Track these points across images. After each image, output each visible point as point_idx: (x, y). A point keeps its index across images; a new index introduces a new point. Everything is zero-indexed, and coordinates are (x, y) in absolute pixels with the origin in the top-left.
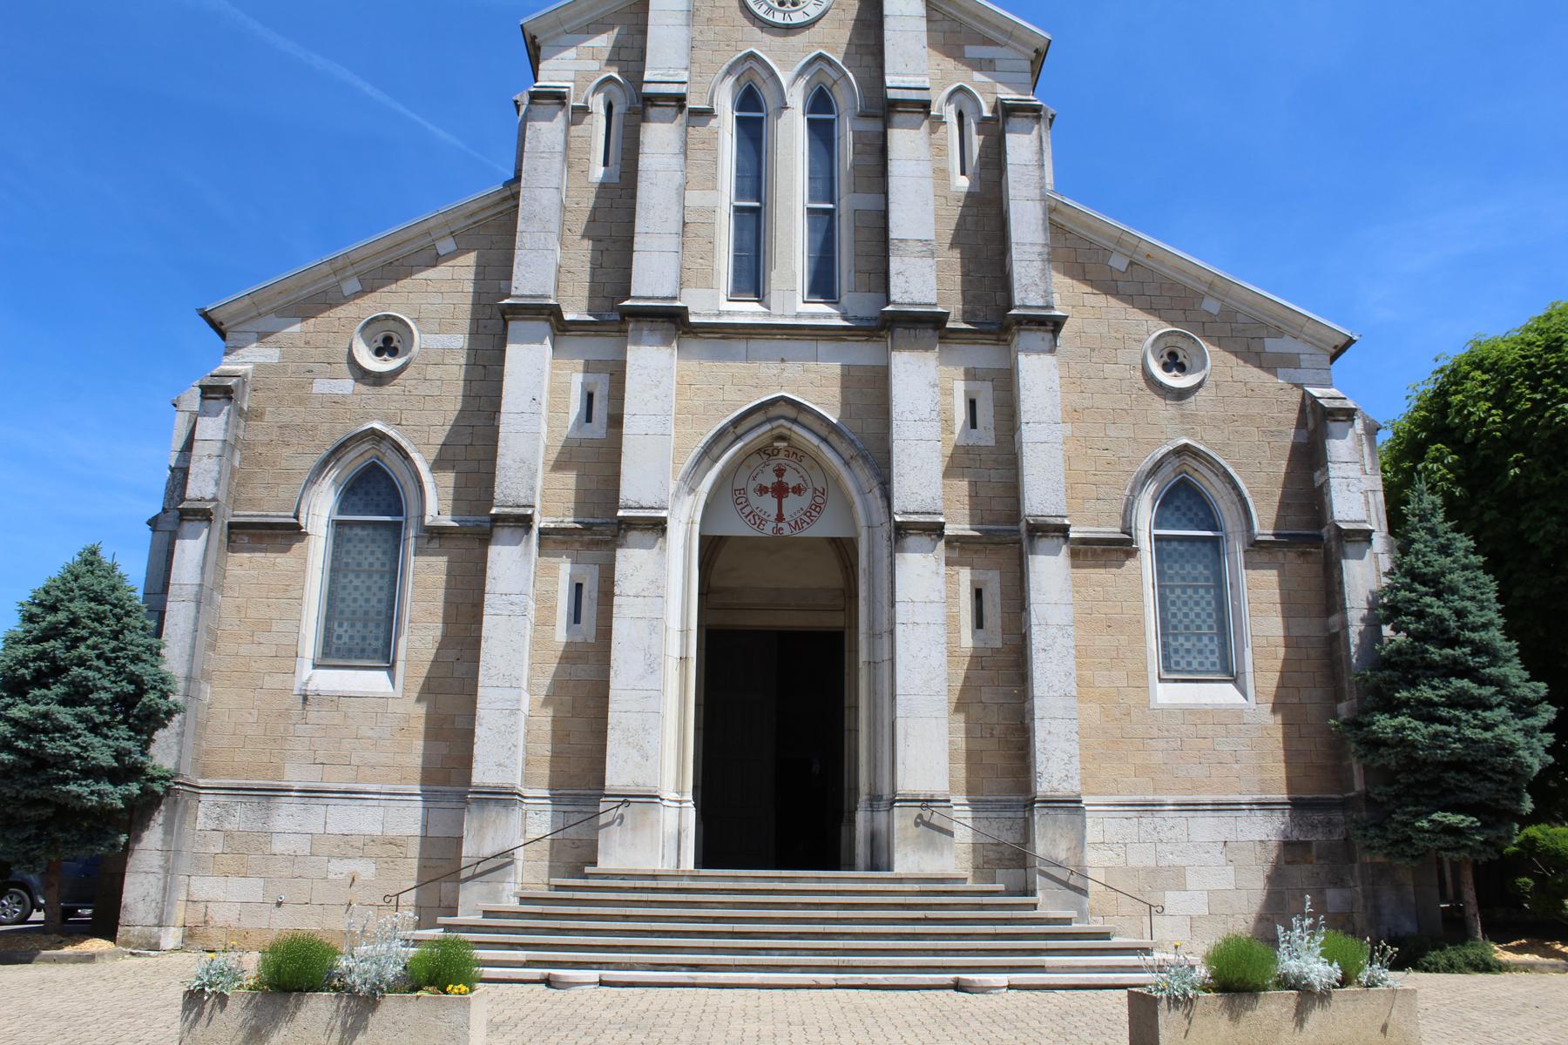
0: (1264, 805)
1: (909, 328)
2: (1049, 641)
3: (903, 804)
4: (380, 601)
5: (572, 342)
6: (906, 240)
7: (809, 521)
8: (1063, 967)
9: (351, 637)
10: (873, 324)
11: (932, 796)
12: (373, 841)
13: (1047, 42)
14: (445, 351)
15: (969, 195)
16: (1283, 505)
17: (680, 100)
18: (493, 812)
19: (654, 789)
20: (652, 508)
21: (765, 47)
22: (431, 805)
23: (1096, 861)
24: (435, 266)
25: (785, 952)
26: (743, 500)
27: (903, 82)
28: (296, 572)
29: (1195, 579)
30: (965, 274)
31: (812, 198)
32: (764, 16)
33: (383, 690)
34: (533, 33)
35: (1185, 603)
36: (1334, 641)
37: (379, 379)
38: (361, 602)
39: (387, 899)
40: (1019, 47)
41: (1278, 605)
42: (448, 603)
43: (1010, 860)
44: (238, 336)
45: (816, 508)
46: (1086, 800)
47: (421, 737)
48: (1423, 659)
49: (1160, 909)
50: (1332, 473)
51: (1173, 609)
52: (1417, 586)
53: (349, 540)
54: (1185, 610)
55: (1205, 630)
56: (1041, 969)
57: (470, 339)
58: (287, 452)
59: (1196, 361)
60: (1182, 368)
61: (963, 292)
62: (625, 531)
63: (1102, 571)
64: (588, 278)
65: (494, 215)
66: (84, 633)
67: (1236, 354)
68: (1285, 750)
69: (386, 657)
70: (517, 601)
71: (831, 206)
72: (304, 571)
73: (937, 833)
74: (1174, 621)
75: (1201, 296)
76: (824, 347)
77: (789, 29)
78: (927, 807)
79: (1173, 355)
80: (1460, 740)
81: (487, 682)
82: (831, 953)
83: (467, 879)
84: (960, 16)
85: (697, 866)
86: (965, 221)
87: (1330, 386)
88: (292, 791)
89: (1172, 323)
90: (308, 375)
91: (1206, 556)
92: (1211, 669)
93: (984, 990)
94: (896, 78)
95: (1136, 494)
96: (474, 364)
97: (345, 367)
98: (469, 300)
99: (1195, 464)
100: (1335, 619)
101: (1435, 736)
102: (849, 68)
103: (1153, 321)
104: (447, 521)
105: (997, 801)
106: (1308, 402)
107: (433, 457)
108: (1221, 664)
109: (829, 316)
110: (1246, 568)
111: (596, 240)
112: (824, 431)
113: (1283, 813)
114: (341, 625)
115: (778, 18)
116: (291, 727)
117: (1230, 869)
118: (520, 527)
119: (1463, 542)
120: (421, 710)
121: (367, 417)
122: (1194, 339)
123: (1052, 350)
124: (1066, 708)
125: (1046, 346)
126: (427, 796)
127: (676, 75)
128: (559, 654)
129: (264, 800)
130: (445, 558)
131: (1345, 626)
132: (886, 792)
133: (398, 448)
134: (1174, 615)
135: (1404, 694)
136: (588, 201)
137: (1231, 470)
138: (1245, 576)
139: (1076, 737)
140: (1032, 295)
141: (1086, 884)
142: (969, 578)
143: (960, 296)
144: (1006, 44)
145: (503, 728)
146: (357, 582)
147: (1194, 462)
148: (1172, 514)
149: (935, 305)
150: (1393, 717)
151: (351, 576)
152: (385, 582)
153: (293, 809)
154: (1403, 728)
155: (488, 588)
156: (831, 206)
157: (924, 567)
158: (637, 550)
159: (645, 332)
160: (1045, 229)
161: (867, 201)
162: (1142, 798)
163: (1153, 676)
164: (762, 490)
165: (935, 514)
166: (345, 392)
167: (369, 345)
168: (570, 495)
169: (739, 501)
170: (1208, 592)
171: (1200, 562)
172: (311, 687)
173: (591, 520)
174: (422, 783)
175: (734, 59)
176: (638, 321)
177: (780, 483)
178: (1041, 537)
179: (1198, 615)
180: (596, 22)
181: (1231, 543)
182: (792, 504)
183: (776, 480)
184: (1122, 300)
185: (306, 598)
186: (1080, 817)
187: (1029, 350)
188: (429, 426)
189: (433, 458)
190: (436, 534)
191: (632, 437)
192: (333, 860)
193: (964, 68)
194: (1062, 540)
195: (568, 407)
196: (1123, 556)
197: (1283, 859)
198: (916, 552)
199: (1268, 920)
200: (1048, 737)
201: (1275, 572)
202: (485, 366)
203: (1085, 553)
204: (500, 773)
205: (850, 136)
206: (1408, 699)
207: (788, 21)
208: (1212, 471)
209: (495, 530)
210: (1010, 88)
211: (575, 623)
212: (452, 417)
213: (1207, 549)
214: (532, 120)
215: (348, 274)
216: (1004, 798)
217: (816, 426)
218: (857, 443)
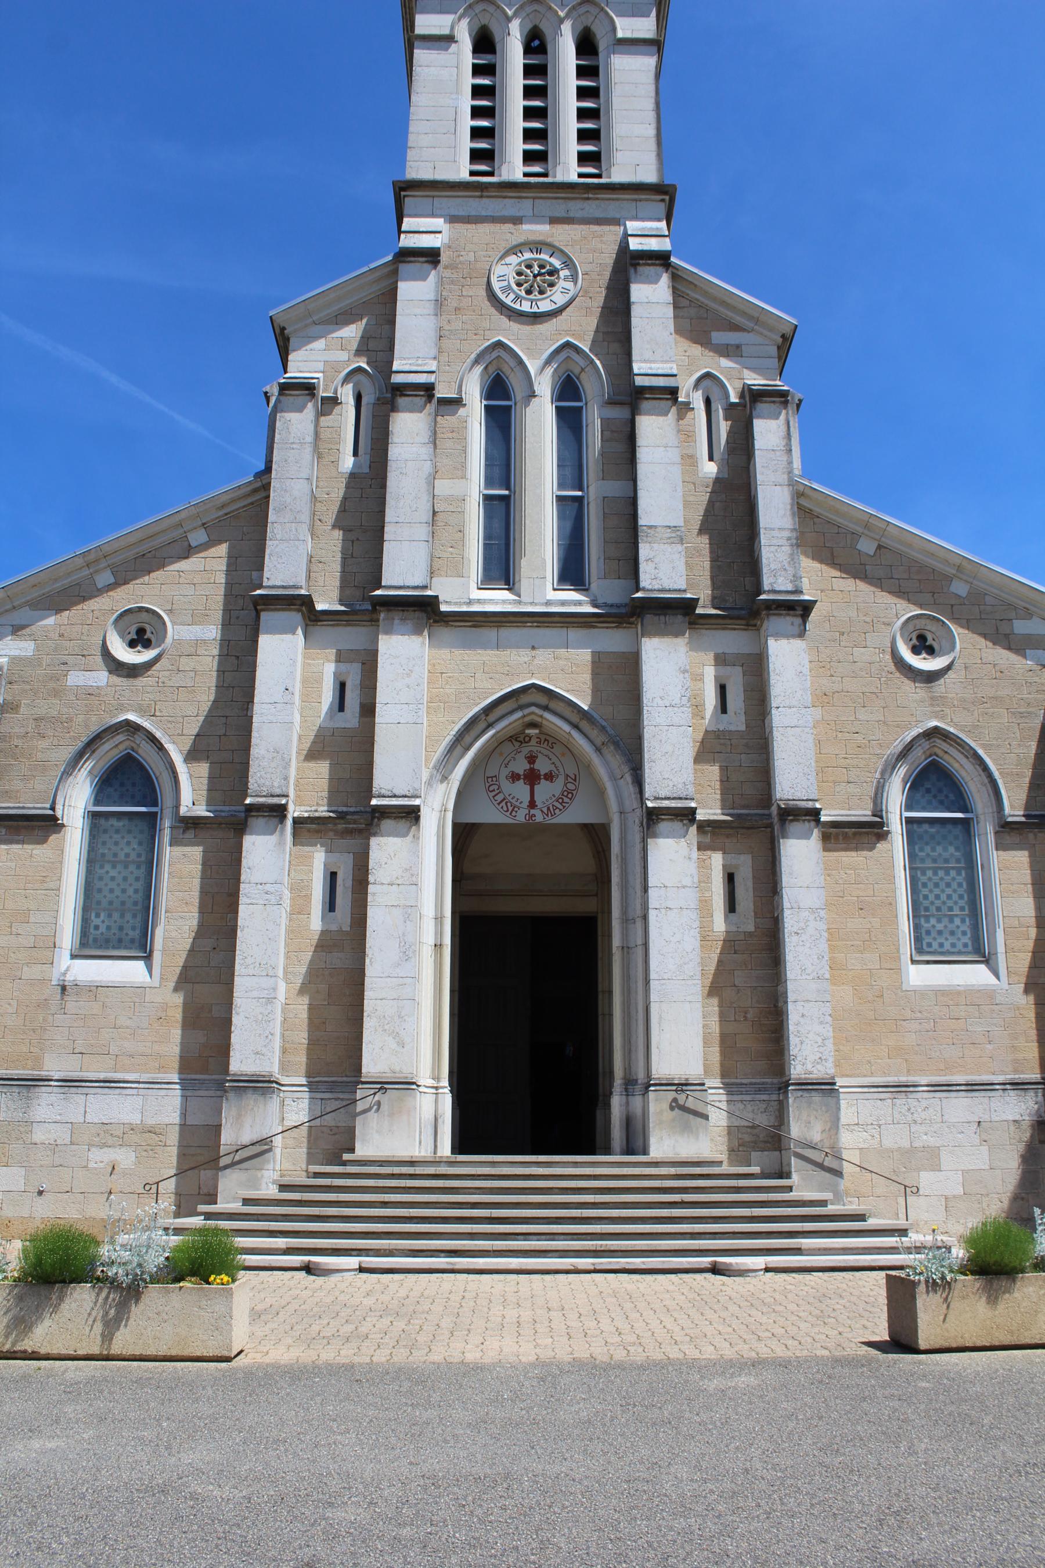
0: (1017, 1085)
1: (659, 615)
2: (802, 925)
3: (658, 1088)
4: (136, 891)
5: (324, 632)
6: (656, 527)
7: (561, 807)
8: (819, 1249)
9: (109, 928)
10: (623, 610)
11: (687, 1079)
12: (132, 1129)
13: (793, 327)
14: (198, 643)
15: (717, 480)
17: (428, 389)
18: (251, 1099)
19: (411, 1076)
20: (405, 796)
21: (512, 334)
22: (189, 1093)
23: (850, 1142)
24: (187, 558)
25: (543, 1237)
26: (496, 787)
27: (651, 368)
28: (53, 863)
29: (946, 861)
30: (713, 560)
31: (561, 485)
32: (512, 305)
33: (141, 980)
34: (282, 325)
35: (936, 885)
37: (132, 671)
38: (118, 892)
39: (148, 1187)
40: (765, 332)
41: (1030, 886)
42: (204, 892)
43: (766, 1142)
45: (567, 796)
46: (840, 1082)
47: (179, 1025)
49: (914, 1190)
51: (925, 891)
53: (105, 831)
55: (956, 911)
56: (798, 1251)
57: (222, 629)
58: (42, 744)
59: (945, 644)
60: (931, 651)
61: (712, 578)
62: (379, 819)
63: (854, 854)
64: (339, 568)
65: (244, 507)
67: (985, 636)
68: (1038, 1030)
69: (143, 946)
70: (272, 890)
71: (579, 493)
72: (61, 862)
73: (691, 1116)
74: (926, 903)
75: (949, 579)
76: (574, 634)
77: (537, 318)
78: (682, 1090)
79: (922, 638)
81: (243, 971)
82: (589, 1237)
83: (226, 1167)
84: (706, 302)
85: (453, 1153)
86: (713, 505)
88: (51, 1080)
90: (63, 667)
91: (956, 837)
92: (963, 950)
93: (742, 1273)
94: (643, 365)
95: (887, 777)
96: (227, 655)
97: (99, 659)
98: (222, 591)
99: (945, 746)
102: (596, 355)
103: (901, 604)
104: (201, 811)
105: (751, 1084)
107: (187, 747)
108: (973, 944)
109: (579, 603)
110: (997, 849)
111: (346, 530)
112: (575, 718)
113: (1036, 1093)
114: (98, 916)
115: (526, 307)
116: (50, 1017)
117: (984, 1149)
118: (274, 816)
120: (179, 999)
121: (122, 709)
122: (943, 622)
123: (801, 634)
124: (818, 991)
125: (796, 630)
126: (186, 1085)
127: (425, 364)
128: (314, 942)
129: (24, 1090)
130: (201, 849)
132: (641, 1076)
134: (926, 897)
136: (338, 491)
137: (981, 752)
139: (829, 1019)
140: (780, 580)
141: (841, 1166)
142: (721, 863)
143: (709, 582)
144: (753, 330)
145: (260, 1017)
146: (113, 873)
147: (944, 744)
148: (923, 796)
149: (685, 591)
152: (141, 872)
153: (53, 1098)
155: (243, 878)
156: (579, 493)
157: (677, 852)
158: (391, 839)
159: (396, 622)
160: (793, 514)
161: (615, 488)
162: (896, 1079)
164: (514, 777)
165: (686, 799)
166: (100, 684)
167: (122, 637)
168: (324, 784)
169: (491, 788)
170: (959, 874)
171: (951, 844)
172: (69, 977)
173: (345, 809)
174: (180, 1072)
175: (482, 347)
176: (391, 610)
177: (532, 770)
178: (792, 821)
179: (949, 897)
180: (345, 313)
181: (981, 824)
182: (545, 791)
183: (527, 767)
184: (871, 584)
185: (63, 889)
186: (835, 1099)
187: (778, 635)
188: (183, 717)
189: (188, 748)
190: (190, 825)
191: (384, 725)
192: (93, 1149)
193: (711, 354)
194: (813, 824)
195: (320, 697)
196: (874, 838)
197: (1037, 1138)
198: (668, 837)
199: (1023, 1199)
200: (802, 1020)
201: (1026, 853)
202: (238, 657)
203: (837, 836)
204: (258, 1061)
205: (598, 423)
207: (535, 310)
208: (963, 753)
209: (250, 819)
210: (755, 372)
211: (330, 911)
212: (205, 707)
213: (958, 830)
214: (282, 411)
215: (102, 566)
216: (758, 1081)
217: (567, 712)
218: (609, 729)
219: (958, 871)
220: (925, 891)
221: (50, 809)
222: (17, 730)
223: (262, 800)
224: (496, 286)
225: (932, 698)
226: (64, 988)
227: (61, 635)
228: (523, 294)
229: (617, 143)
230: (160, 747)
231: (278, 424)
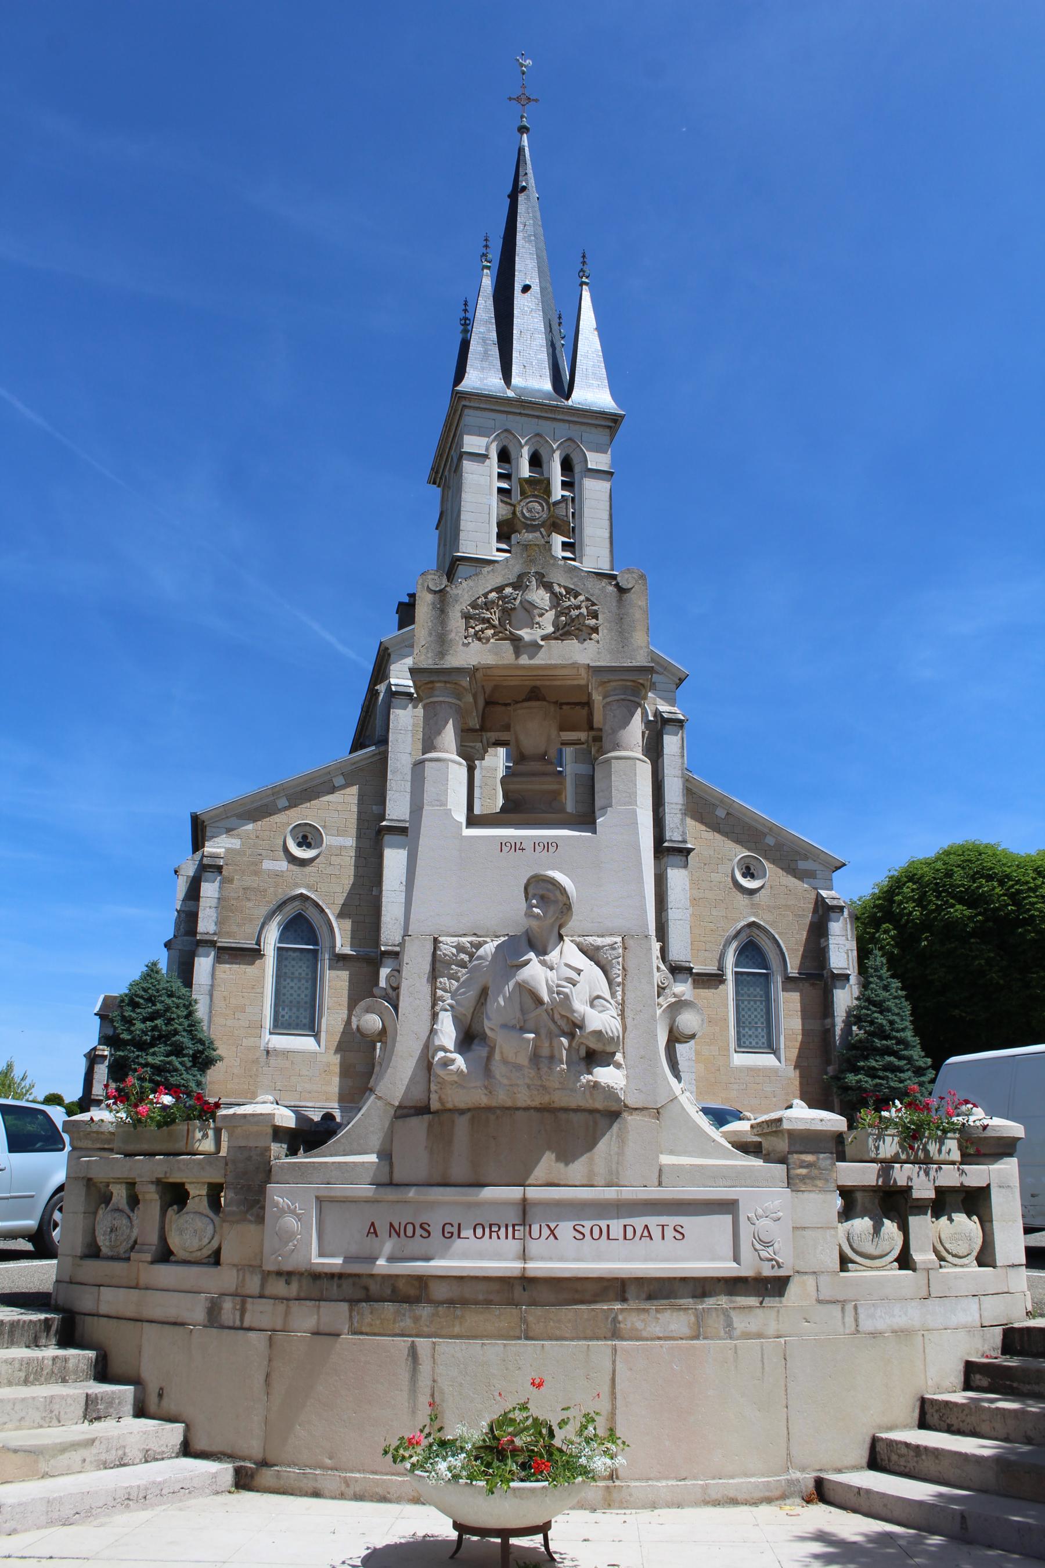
4: (306, 996)
9: (290, 1017)
14: (341, 848)
16: (803, 957)
22: (344, 1114)
29: (755, 996)
35: (749, 1009)
36: (827, 1033)
37: (303, 863)
38: (295, 996)
44: (214, 830)
48: (872, 1045)
50: (831, 942)
51: (743, 1013)
52: (871, 1007)
53: (286, 959)
54: (749, 1013)
55: (759, 1025)
58: (250, 904)
60: (752, 876)
63: (707, 991)
66: (174, 1016)
67: (782, 869)
69: (312, 1029)
74: (743, 1019)
75: (765, 835)
79: (748, 868)
80: (888, 1088)
87: (831, 889)
89: (749, 850)
90: (259, 857)
97: (282, 853)
98: (355, 816)
100: (828, 1021)
101: (876, 1085)
103: (738, 848)
104: (347, 950)
106: (820, 899)
114: (283, 1009)
119: (896, 983)
121: (297, 885)
123: (686, 866)
125: (682, 864)
130: (348, 972)
131: (833, 1025)
133: (317, 905)
134: (743, 1016)
135: (862, 1064)
137: (777, 936)
138: (782, 995)
144: (663, 674)
146: (292, 984)
150: (856, 1075)
151: (288, 980)
152: (309, 985)
154: (860, 1081)
160: (683, 795)
161: (583, 769)
170: (761, 1004)
172: (271, 1046)
184: (722, 835)
185: (265, 993)
201: (798, 994)
203: (698, 980)
206: (864, 1066)
209: (384, 959)
212: (348, 888)
213: (762, 979)
219: (761, 1002)
220: (743, 1013)
221: (256, 944)
222: (232, 894)
223: (390, 948)
225: (752, 904)
226: (268, 1052)
227: (257, 837)
229: (587, 540)
230: (322, 911)
231: (391, 717)
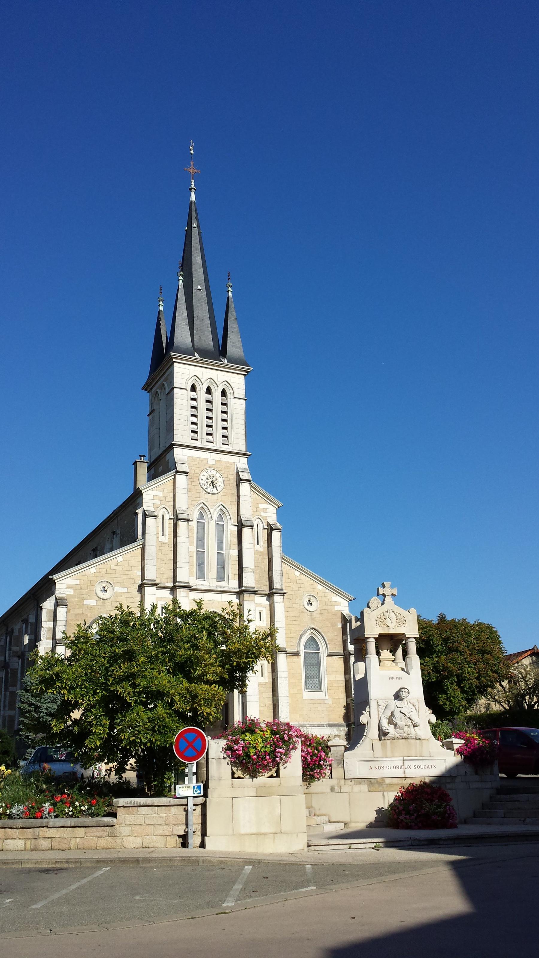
51: (308, 672)
74: (308, 675)
134: (308, 674)
140: (278, 585)
163: (303, 690)
179: (313, 674)
220: (308, 672)
224: (201, 482)
228: (208, 486)
